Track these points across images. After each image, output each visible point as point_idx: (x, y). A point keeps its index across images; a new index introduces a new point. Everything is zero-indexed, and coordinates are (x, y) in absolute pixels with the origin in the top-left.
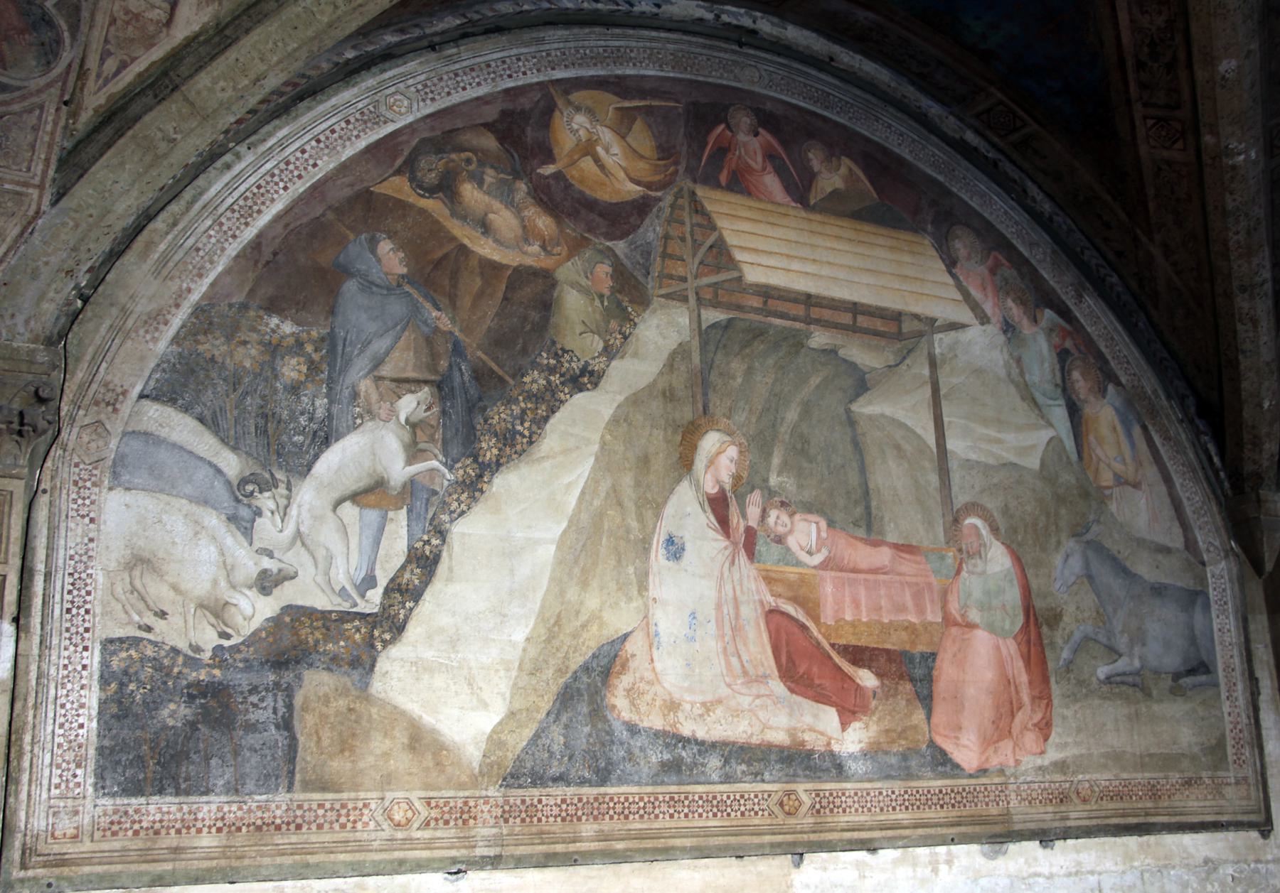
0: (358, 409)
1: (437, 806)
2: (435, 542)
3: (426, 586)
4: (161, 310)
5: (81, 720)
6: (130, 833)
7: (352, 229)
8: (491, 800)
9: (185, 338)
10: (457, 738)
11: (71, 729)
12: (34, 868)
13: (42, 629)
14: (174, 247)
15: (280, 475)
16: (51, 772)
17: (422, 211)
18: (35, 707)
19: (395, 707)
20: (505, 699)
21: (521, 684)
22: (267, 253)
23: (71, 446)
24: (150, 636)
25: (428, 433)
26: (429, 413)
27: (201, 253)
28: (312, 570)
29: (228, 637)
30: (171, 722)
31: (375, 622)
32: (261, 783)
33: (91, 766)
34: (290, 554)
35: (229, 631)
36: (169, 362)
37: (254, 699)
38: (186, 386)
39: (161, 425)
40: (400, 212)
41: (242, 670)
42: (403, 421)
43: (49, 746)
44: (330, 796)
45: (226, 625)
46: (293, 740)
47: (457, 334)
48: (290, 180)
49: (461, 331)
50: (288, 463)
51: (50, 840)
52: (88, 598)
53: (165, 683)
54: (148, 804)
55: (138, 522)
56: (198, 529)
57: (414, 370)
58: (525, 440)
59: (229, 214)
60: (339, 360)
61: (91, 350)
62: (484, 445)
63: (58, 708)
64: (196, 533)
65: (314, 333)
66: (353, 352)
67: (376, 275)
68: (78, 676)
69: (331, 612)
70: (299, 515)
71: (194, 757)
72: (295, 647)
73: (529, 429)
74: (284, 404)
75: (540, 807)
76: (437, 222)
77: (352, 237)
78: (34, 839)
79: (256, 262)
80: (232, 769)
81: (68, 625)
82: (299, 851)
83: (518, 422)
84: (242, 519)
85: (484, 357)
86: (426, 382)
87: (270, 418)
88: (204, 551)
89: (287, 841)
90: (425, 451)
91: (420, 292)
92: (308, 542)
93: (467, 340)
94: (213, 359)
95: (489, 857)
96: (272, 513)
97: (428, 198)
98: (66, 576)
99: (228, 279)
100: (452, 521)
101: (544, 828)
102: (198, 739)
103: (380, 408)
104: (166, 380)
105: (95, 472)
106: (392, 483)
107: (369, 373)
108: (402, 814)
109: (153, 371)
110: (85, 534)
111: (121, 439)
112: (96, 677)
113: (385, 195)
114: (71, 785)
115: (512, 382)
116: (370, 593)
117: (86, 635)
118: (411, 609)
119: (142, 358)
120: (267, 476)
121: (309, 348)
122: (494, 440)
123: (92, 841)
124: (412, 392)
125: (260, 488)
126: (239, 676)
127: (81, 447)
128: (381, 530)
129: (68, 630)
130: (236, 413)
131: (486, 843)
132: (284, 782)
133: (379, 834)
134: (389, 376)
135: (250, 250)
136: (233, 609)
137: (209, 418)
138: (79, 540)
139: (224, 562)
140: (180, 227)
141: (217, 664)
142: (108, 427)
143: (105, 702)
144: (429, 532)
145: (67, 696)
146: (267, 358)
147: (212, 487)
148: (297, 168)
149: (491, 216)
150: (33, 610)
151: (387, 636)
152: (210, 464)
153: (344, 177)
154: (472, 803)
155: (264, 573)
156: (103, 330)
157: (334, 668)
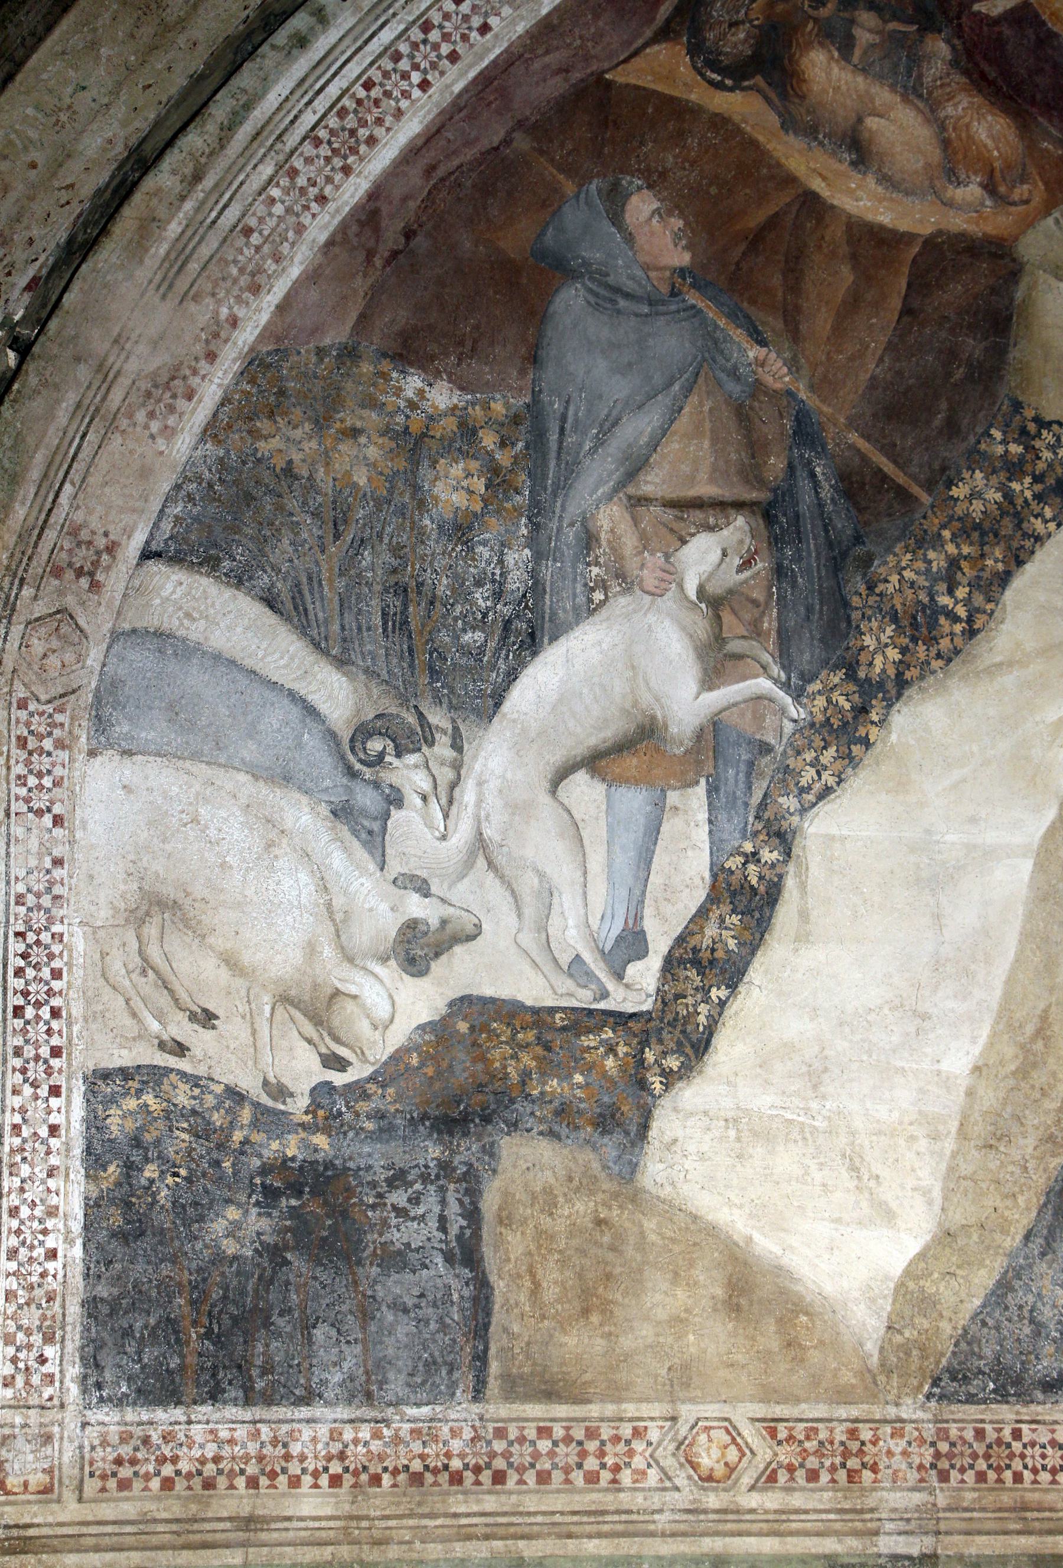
0: (595, 570)
1: (790, 1438)
2: (769, 856)
3: (753, 953)
4: (177, 368)
5: (50, 1242)
6: (155, 1484)
7: (569, 170)
8: (909, 1427)
9: (230, 426)
10: (829, 1288)
14: (196, 229)
15: (437, 718)
17: (720, 122)
19: (695, 1218)
20: (930, 1203)
21: (966, 1169)
22: (391, 236)
24: (183, 1065)
25: (747, 617)
26: (747, 574)
27: (255, 239)
28: (510, 920)
29: (341, 1065)
30: (230, 1247)
31: (646, 1032)
32: (419, 1380)
33: (74, 1339)
34: (463, 886)
35: (343, 1052)
36: (199, 479)
37: (399, 1198)
38: (236, 530)
39: (188, 615)
40: (671, 126)
41: (371, 1136)
42: (692, 592)
44: (562, 1410)
45: (337, 1040)
46: (482, 1285)
47: (803, 395)
48: (434, 66)
49: (812, 388)
50: (452, 691)
52: (56, 985)
53: (217, 1164)
54: (189, 1422)
55: (151, 824)
56: (273, 835)
57: (712, 480)
58: (958, 628)
59: (308, 149)
60: (552, 464)
61: (40, 458)
62: (869, 641)
64: (270, 845)
65: (498, 407)
66: (580, 445)
67: (623, 274)
68: (42, 1149)
69: (552, 1010)
70: (480, 801)
71: (281, 1322)
72: (480, 1087)
73: (967, 602)
74: (440, 563)
75: (1017, 1446)
76: (754, 143)
77: (569, 188)
79: (370, 254)
80: (358, 1349)
81: (19, 1041)
82: (501, 1531)
83: (942, 587)
84: (364, 813)
85: (863, 445)
86: (739, 505)
87: (412, 595)
88: (287, 883)
89: (475, 1508)
90: (739, 657)
91: (720, 305)
92: (500, 860)
93: (826, 409)
94: (289, 471)
95: (909, 1558)
96: (424, 798)
97: (731, 90)
98: (11, 938)
99: (313, 295)
100: (803, 810)
101: (1030, 1496)
102: (288, 1283)
103: (643, 566)
104: (196, 519)
105: (59, 718)
106: (674, 730)
107: (616, 490)
108: (716, 1453)
109: (168, 500)
111: (109, 647)
112: (78, 1151)
113: (637, 88)
114: (36, 1380)
115: (926, 499)
116: (633, 970)
117: (55, 1063)
118: (722, 1004)
119: (145, 473)
120: (411, 719)
121: (489, 440)
122: (889, 630)
123: (80, 1500)
124: (711, 529)
125: (396, 747)
126: (367, 1149)
128: (654, 831)
129: (18, 1052)
130: (341, 584)
131: (902, 1526)
132: (466, 1379)
133: (671, 1497)
134: (660, 494)
135: (355, 228)
136: (350, 1006)
137: (286, 597)
138: (33, 862)
139: (329, 906)
140: (208, 182)
141: (321, 1122)
142: (82, 622)
144: (756, 834)
145: (22, 1190)
146: (402, 464)
147: (299, 746)
148: (446, 37)
149: (872, 123)
151: (673, 1063)
152: (293, 696)
153: (547, 52)
154: (866, 1435)
155: (411, 928)
156: (62, 416)
157: (564, 1131)
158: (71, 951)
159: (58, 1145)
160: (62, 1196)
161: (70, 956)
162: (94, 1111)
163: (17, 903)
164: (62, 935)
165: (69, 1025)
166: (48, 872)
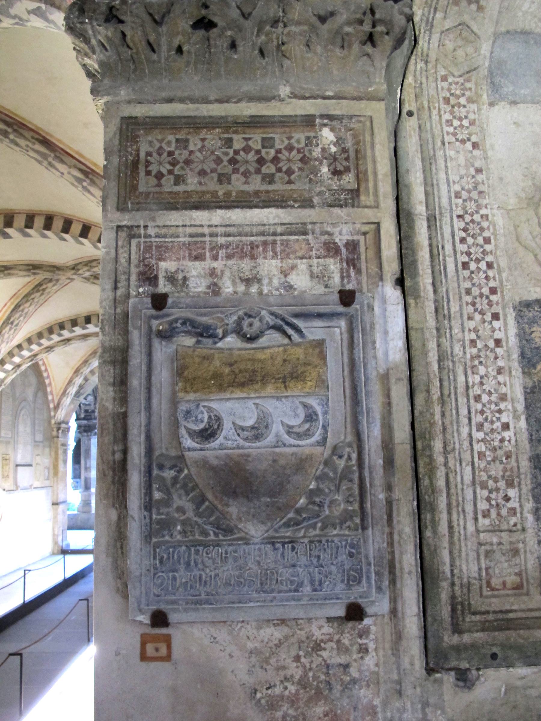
5: (504, 418)
11: (493, 431)
12: (469, 631)
13: (435, 291)
16: (475, 493)
18: (442, 401)
23: (433, 56)
33: (527, 485)
43: (467, 456)
51: (486, 592)
52: (488, 247)
63: (472, 401)
68: (492, 355)
78: (465, 590)
81: (468, 285)
105: (468, 85)
110: (469, 163)
111: (494, 42)
112: (515, 356)
114: (504, 512)
117: (493, 298)
127: (446, 56)
129: (468, 292)
138: (463, 172)
142: (475, 28)
143: (533, 392)
145: (482, 384)
150: (420, 267)
158: (494, 226)
159: (502, 353)
160: (508, 386)
161: (495, 229)
162: (523, 329)
163: (456, 197)
164: (487, 216)
165: (500, 273)
166: (473, 177)
